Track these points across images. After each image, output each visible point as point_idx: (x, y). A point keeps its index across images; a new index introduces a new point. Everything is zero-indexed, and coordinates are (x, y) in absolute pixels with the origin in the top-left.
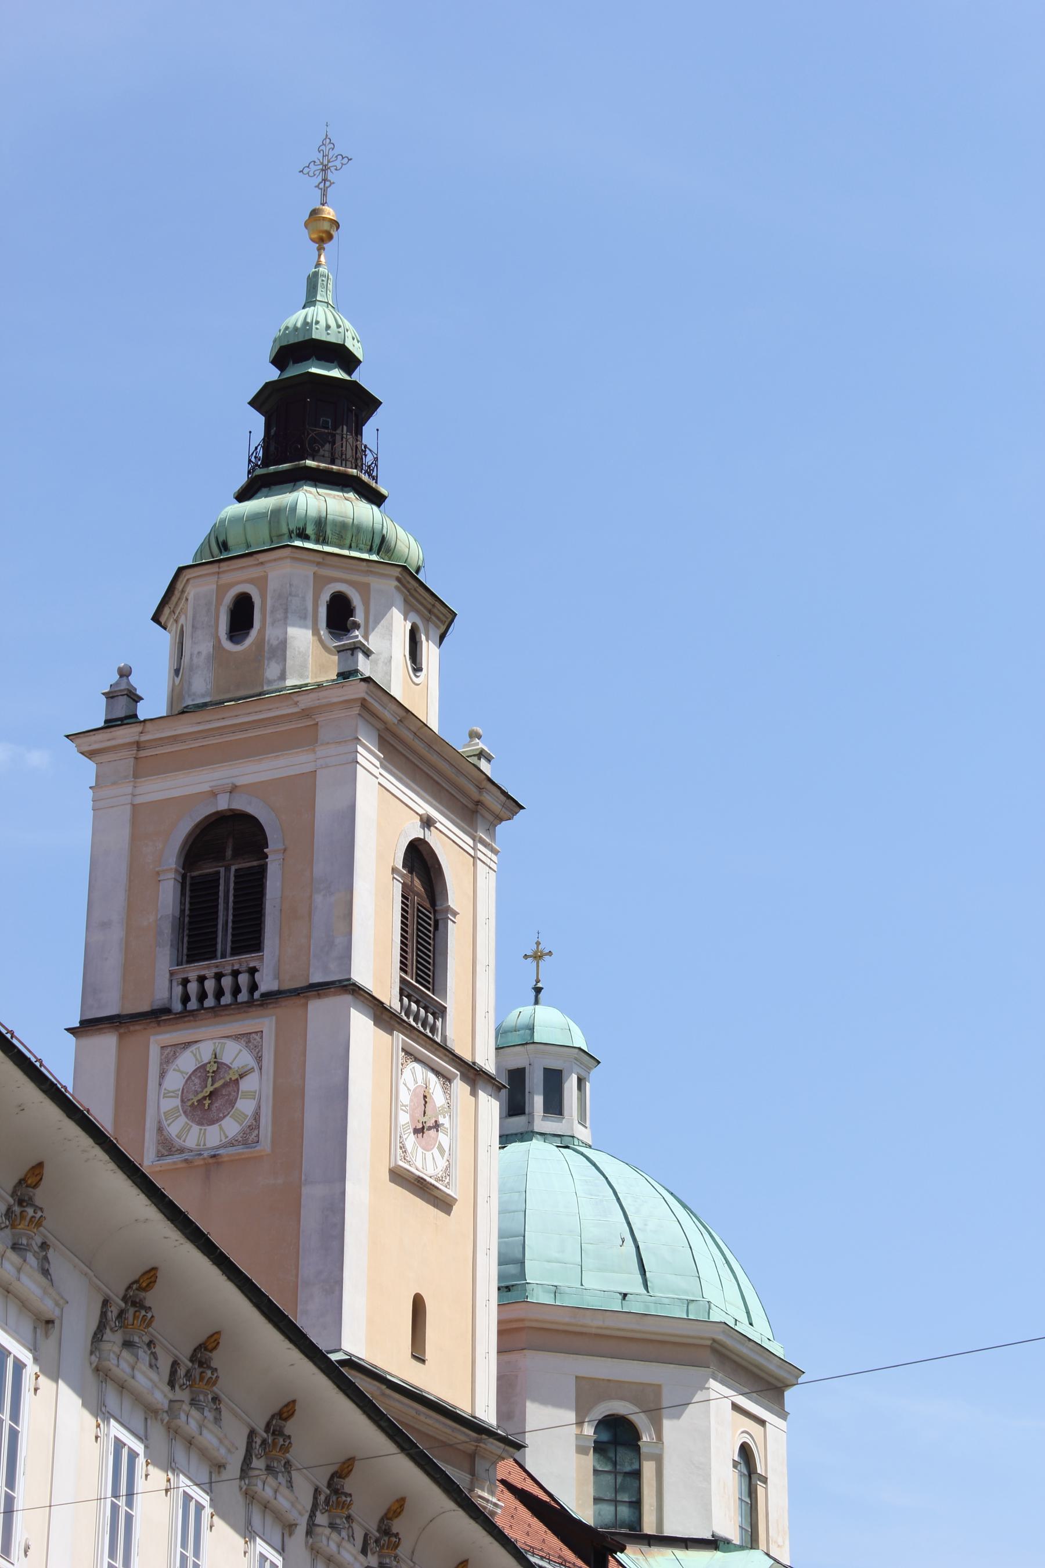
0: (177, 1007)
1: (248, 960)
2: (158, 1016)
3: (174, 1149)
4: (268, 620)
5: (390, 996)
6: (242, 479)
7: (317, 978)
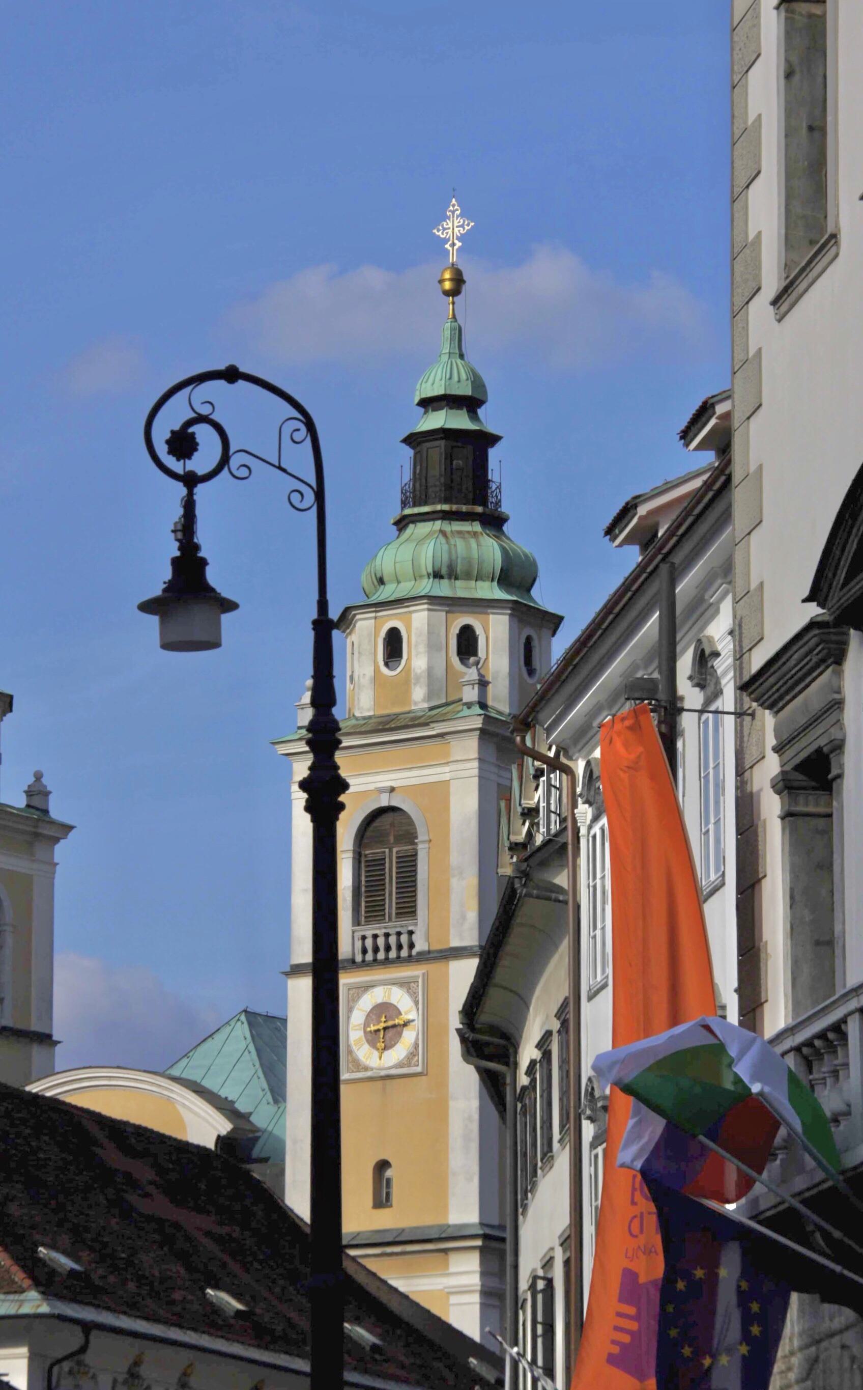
0: (359, 958)
1: (406, 924)
3: (361, 1067)
4: (413, 653)
6: (396, 513)
7: (455, 943)
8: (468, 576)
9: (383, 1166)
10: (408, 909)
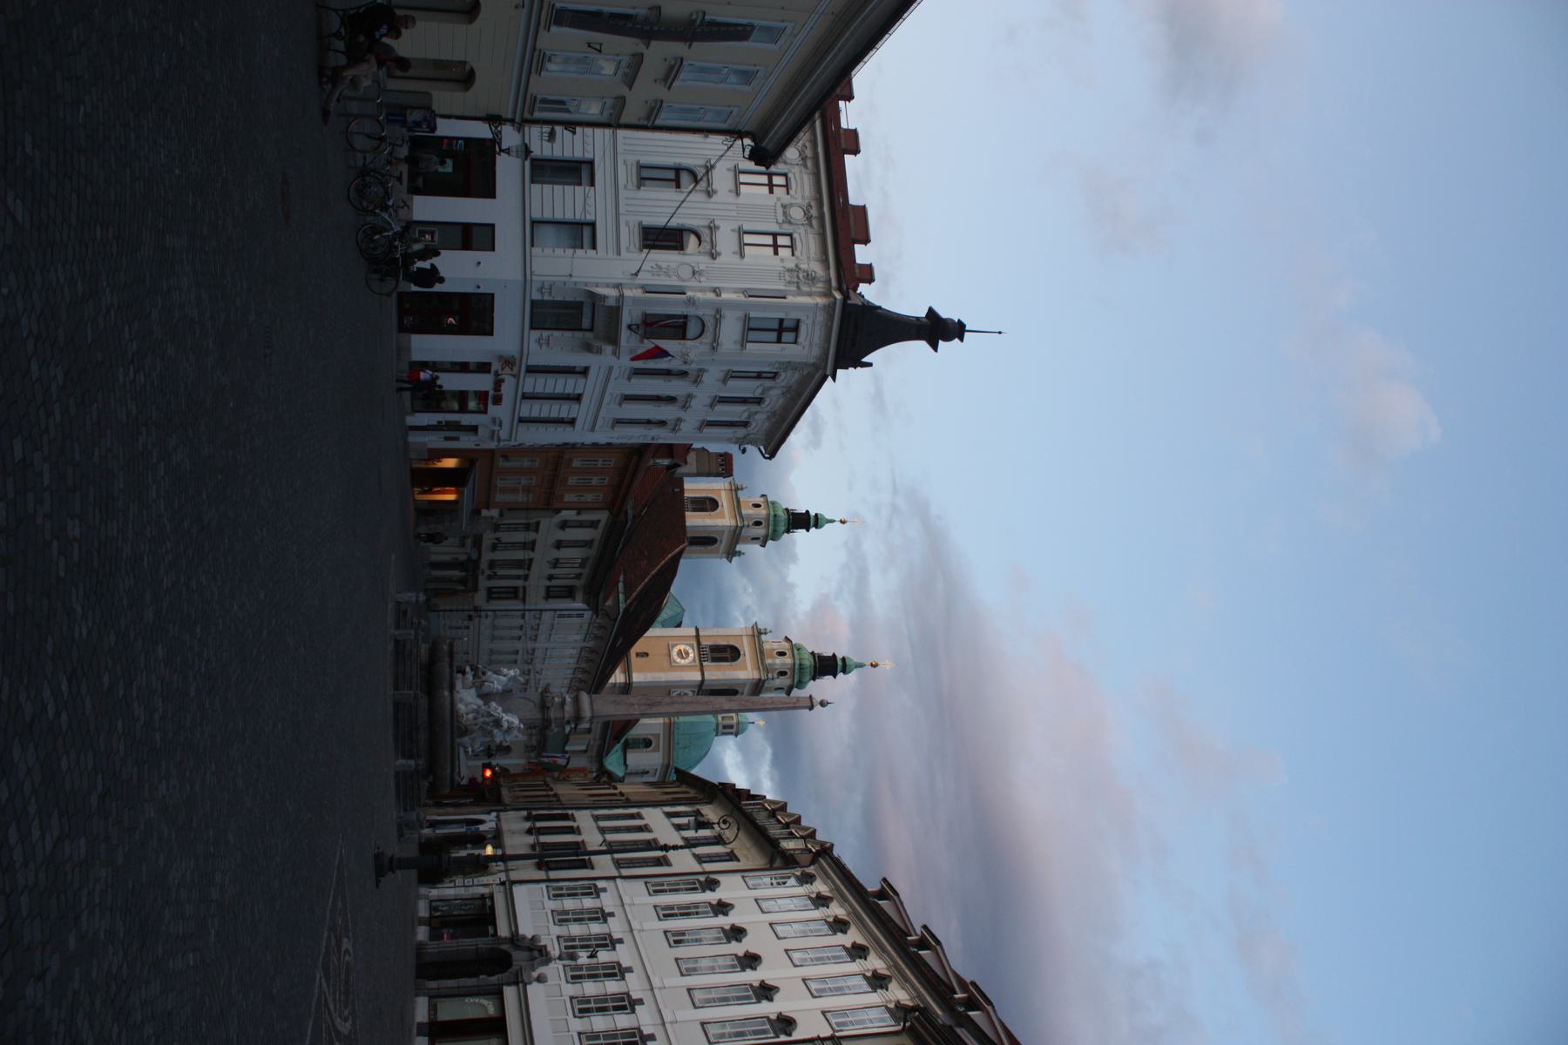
2: (699, 643)
5: (704, 688)
6: (816, 652)
8: (800, 672)
9: (647, 655)
10: (714, 660)
